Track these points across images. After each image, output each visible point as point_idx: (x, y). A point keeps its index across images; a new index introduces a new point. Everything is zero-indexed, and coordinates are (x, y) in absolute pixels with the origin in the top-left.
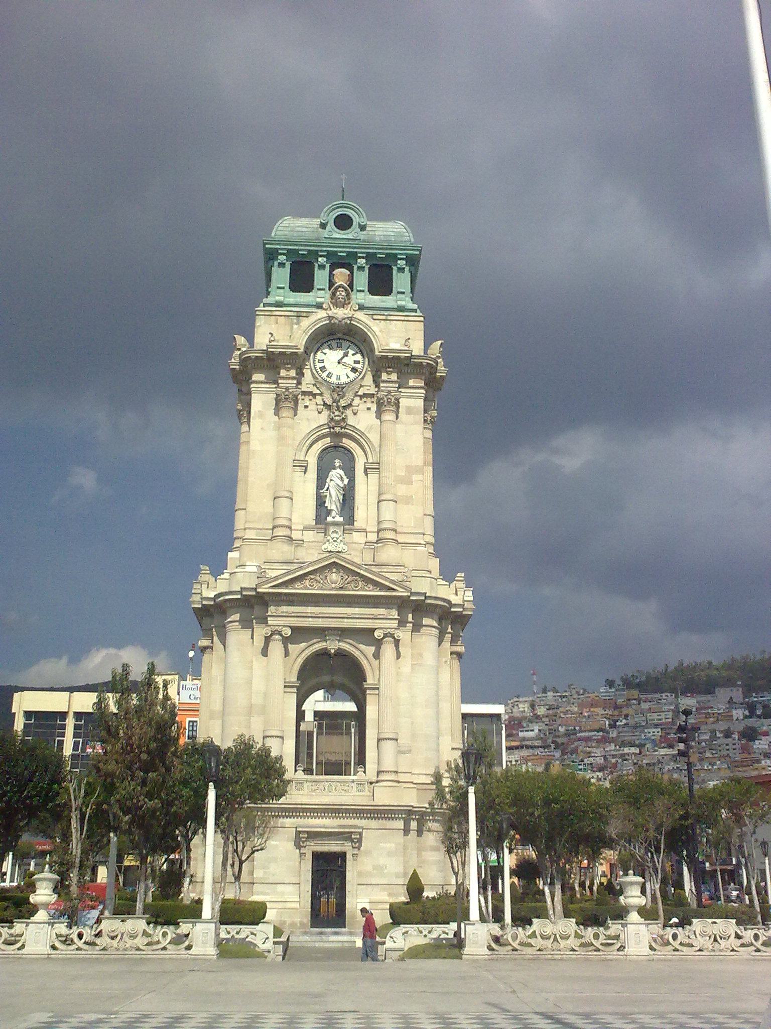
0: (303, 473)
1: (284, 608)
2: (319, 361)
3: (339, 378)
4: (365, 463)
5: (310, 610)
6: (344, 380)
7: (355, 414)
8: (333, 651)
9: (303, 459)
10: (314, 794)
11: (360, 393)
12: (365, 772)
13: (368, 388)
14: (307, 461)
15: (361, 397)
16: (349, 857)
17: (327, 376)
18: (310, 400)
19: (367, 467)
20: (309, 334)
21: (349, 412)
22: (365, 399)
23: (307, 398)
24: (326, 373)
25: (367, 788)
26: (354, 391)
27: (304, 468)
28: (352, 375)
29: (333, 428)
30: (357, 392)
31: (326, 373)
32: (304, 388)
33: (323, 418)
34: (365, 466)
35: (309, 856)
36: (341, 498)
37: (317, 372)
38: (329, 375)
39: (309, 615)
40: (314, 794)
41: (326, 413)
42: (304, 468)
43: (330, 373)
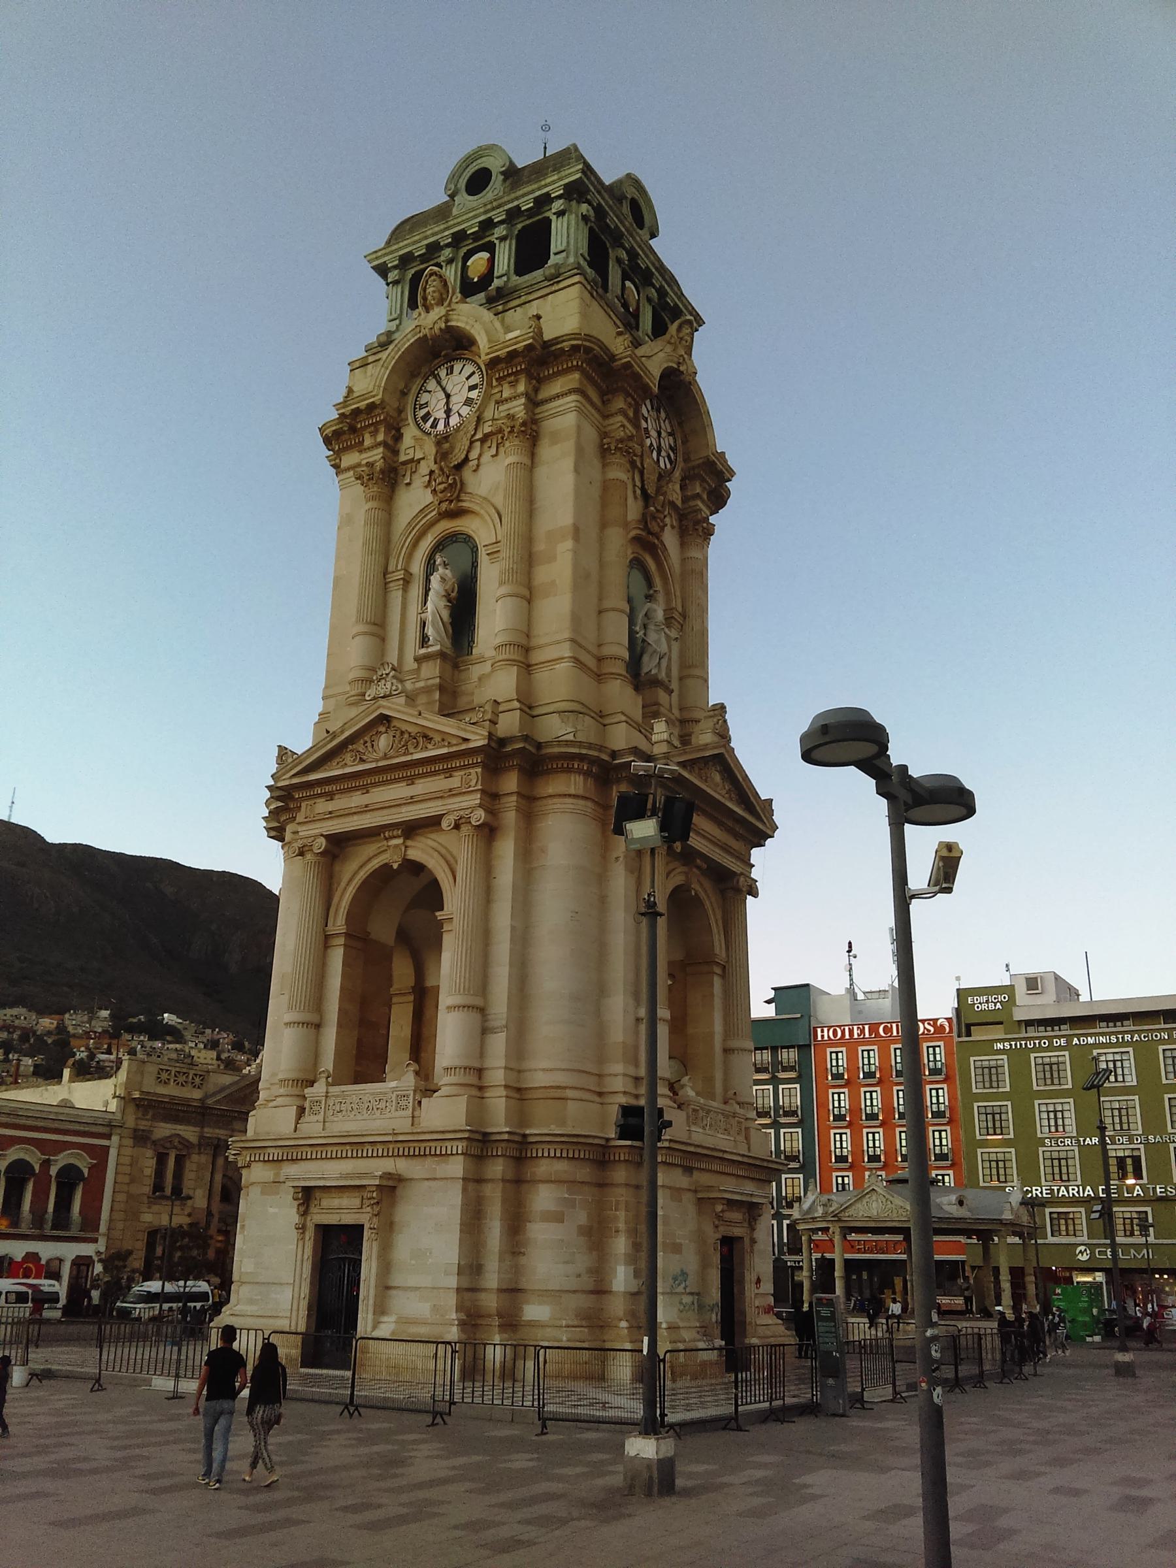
0: (400, 592)
1: (322, 806)
2: (422, 407)
5: (357, 800)
8: (395, 866)
10: (336, 1119)
11: (477, 437)
15: (483, 440)
17: (431, 427)
20: (390, 368)
21: (467, 473)
26: (469, 436)
27: (401, 582)
28: (465, 411)
31: (432, 419)
35: (310, 1233)
36: (446, 614)
39: (354, 810)
40: (336, 1119)
42: (401, 582)
43: (435, 419)
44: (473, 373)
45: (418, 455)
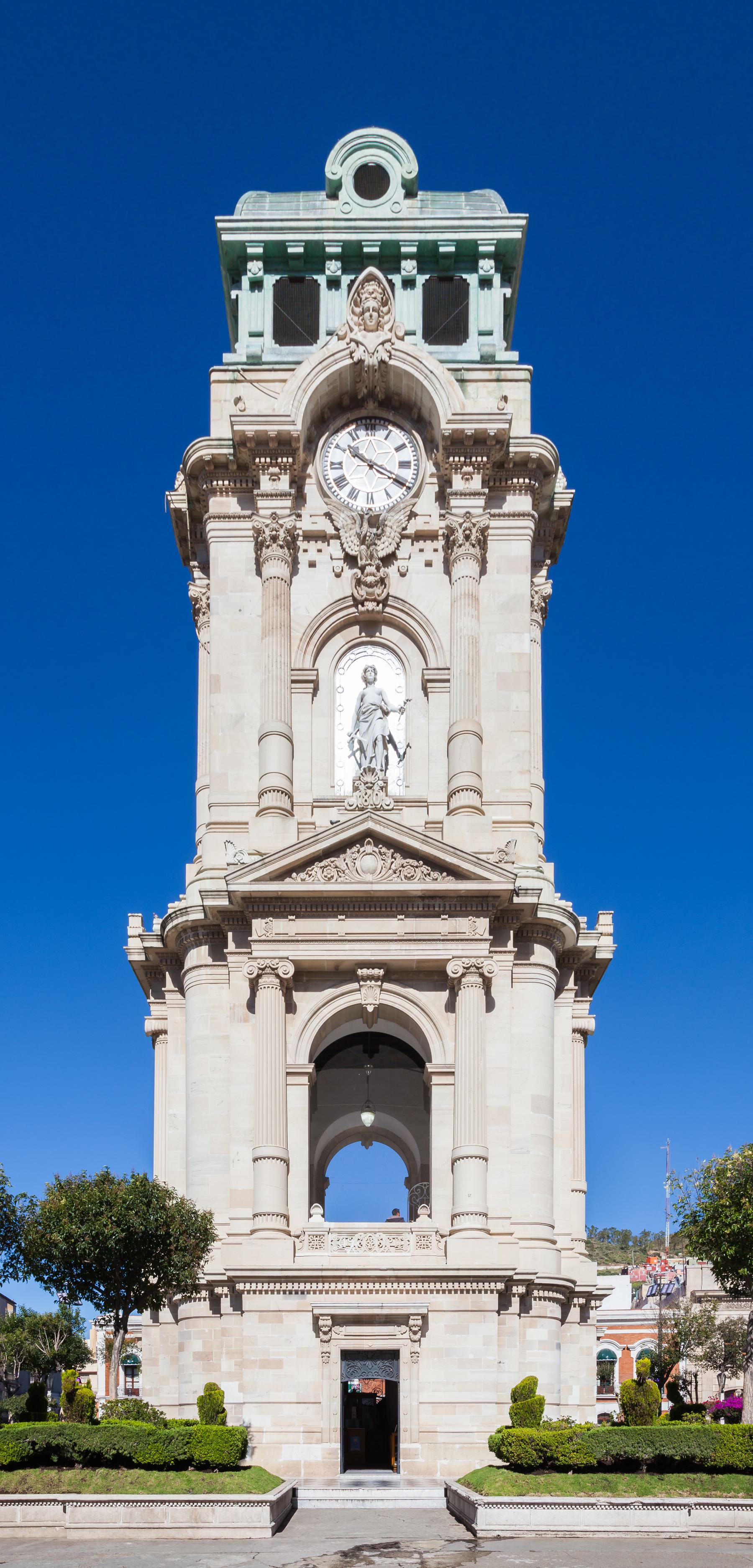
3: (370, 498)
4: (423, 669)
6: (380, 504)
7: (403, 575)
9: (311, 667)
12: (430, 1216)
13: (427, 519)
14: (317, 670)
16: (404, 1356)
18: (320, 551)
19: (426, 677)
21: (392, 571)
22: (421, 544)
23: (312, 546)
24: (347, 489)
25: (434, 1242)
29: (363, 605)
30: (404, 529)
31: (347, 489)
32: (306, 524)
33: (345, 586)
34: (423, 675)
37: (330, 488)
38: (353, 494)
41: (349, 573)
44: (403, 446)
45: (331, 531)
